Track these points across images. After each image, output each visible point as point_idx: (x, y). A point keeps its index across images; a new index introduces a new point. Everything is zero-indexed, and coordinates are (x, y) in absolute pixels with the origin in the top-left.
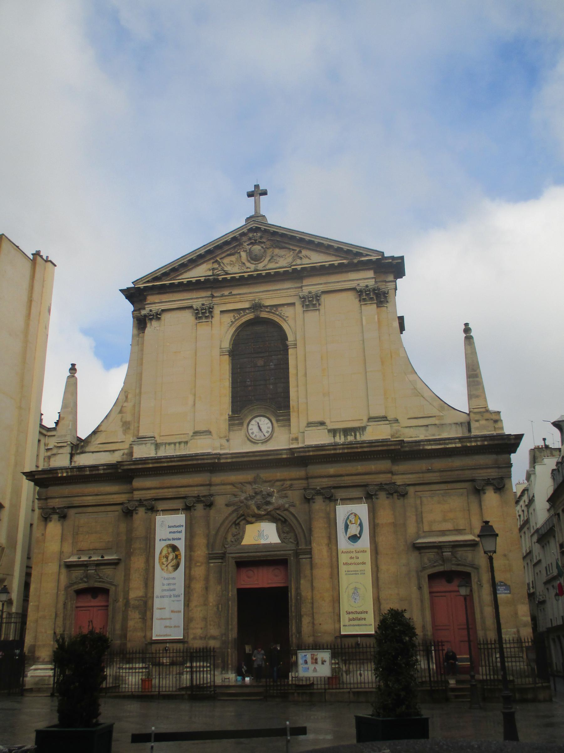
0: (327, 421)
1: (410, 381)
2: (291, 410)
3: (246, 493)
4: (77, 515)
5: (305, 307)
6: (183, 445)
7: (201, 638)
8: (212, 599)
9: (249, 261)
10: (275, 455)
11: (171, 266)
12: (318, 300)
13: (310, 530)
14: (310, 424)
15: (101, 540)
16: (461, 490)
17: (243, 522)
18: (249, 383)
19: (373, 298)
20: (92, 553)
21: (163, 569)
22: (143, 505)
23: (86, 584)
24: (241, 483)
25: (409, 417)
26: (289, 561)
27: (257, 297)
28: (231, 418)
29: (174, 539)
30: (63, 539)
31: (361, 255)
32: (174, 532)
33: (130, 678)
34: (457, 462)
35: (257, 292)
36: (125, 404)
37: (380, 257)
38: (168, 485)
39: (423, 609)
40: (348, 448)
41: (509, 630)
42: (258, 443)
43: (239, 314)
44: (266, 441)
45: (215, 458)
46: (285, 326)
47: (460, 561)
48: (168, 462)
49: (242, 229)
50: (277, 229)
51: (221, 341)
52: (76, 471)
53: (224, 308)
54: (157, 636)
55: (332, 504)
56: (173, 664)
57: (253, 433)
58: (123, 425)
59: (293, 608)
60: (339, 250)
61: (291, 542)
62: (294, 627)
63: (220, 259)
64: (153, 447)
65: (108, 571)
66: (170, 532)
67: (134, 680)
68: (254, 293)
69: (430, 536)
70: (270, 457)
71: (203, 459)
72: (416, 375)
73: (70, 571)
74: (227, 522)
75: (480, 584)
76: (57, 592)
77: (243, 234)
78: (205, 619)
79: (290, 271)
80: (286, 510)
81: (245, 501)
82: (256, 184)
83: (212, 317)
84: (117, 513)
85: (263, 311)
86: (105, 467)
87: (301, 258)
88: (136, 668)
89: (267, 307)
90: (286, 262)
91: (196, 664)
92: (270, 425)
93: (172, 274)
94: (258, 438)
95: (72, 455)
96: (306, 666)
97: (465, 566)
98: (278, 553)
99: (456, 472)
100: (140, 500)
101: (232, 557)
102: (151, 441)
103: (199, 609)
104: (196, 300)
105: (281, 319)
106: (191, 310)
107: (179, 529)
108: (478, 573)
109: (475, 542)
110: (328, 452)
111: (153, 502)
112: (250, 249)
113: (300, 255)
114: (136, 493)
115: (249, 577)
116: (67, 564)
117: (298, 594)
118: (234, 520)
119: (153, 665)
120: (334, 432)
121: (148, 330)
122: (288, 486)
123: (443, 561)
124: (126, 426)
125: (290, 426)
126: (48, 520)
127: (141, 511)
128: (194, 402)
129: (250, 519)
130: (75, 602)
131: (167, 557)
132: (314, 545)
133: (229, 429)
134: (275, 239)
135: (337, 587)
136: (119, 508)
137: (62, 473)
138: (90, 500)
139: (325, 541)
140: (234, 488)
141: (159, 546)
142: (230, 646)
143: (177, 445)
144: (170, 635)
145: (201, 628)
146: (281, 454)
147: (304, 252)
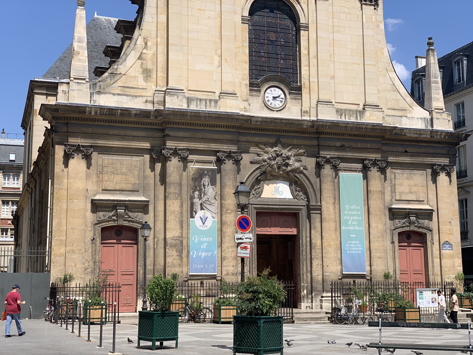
7: (233, 274)
15: (127, 182)
28: (251, 85)
36: (145, 51)
39: (394, 258)
41: (450, 276)
42: (274, 111)
47: (421, 224)
58: (143, 72)
59: (304, 253)
61: (302, 199)
62: (304, 267)
64: (185, 101)
74: (252, 176)
81: (268, 161)
92: (283, 96)
94: (273, 106)
101: (254, 208)
103: (231, 250)
108: (432, 234)
132: (323, 203)
139: (332, 201)
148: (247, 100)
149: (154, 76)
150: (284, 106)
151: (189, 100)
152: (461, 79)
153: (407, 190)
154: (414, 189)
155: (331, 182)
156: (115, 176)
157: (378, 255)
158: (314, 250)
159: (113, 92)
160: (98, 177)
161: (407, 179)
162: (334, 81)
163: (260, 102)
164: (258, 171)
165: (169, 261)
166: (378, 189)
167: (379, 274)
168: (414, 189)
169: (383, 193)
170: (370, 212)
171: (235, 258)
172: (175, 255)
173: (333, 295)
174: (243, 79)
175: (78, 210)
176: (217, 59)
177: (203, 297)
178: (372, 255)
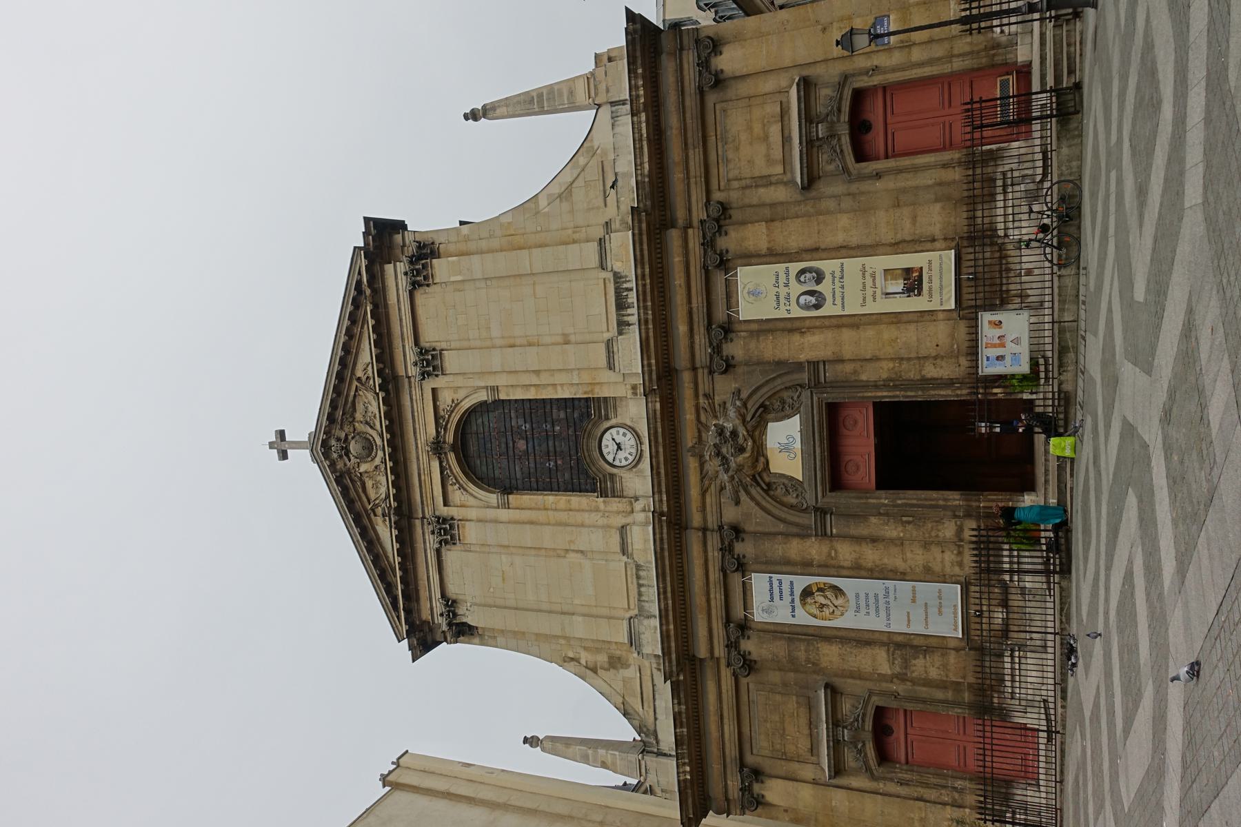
0: (607, 336)
1: (549, 204)
2: (590, 396)
3: (717, 472)
4: (755, 751)
5: (436, 373)
6: (642, 573)
7: (960, 553)
8: (892, 531)
9: (373, 460)
10: (656, 422)
11: (376, 581)
12: (427, 351)
13: (779, 363)
14: (611, 366)
16: (718, 112)
17: (765, 475)
18: (552, 463)
19: (423, 264)
21: (842, 615)
22: (736, 642)
23: (867, 746)
24: (702, 479)
25: (603, 205)
26: (830, 401)
28: (604, 494)
29: (792, 594)
31: (359, 283)
32: (781, 592)
33: (1029, 680)
34: (672, 121)
36: (583, 662)
37: (362, 252)
38: (704, 599)
39: (915, 169)
40: (645, 300)
43: (449, 476)
45: (660, 521)
46: (466, 405)
47: (833, 107)
48: (666, 598)
49: (325, 467)
50: (323, 415)
51: (488, 507)
52: (683, 749)
53: (440, 500)
54: (956, 630)
55: (737, 327)
56: (1005, 604)
57: (626, 459)
58: (614, 668)
59: (909, 393)
60: (353, 319)
61: (798, 397)
62: (942, 393)
64: (646, 622)
65: (846, 706)
66: (781, 599)
67: (1034, 674)
68: (417, 452)
69: (791, 163)
70: (660, 430)
71: (662, 539)
72: (540, 196)
73: (845, 770)
74: (764, 503)
75: (873, 70)
76: (881, 794)
77: (333, 465)
78: (926, 545)
79: (384, 394)
80: (745, 405)
81: (730, 473)
82: (268, 446)
83: (452, 519)
84: (751, 686)
85: (445, 438)
86: (676, 701)
88: (1013, 669)
89: (438, 432)
91: (1006, 563)
92: (613, 431)
93: (389, 579)
94: (634, 451)
95: (660, 754)
96: (1008, 359)
97: (841, 98)
98: (816, 419)
99: (689, 121)
100: (727, 646)
101: (823, 496)
102: (636, 625)
103: (909, 555)
104: (428, 544)
105: (455, 411)
106: (443, 550)
107: (776, 584)
108: (853, 75)
109: (802, 83)
110: (651, 334)
111: (732, 625)
112: (356, 458)
113: (364, 379)
114: (717, 654)
115: (858, 468)
116: (833, 774)
117: (886, 385)
118: (761, 492)
119: (1007, 638)
120: (622, 325)
121: (470, 620)
122: (706, 402)
123: (832, 136)
124: (616, 663)
125: (615, 398)
126: (761, 799)
127: (748, 645)
128: (577, 551)
129: (760, 467)
130: (897, 766)
131: (822, 606)
132: (803, 357)
133: (620, 497)
134: (340, 418)
135: (874, 317)
136: (744, 681)
137: (685, 772)
138: (730, 729)
139: (796, 338)
140: (709, 491)
141: (803, 617)
142: (974, 504)
143: (641, 582)
144: (955, 606)
145: (943, 552)
146: (655, 411)
147: (359, 373)
148: (631, 503)
151: (642, 613)
153: (762, 149)
154: (757, 128)
155: (758, 341)
156: (787, 733)
157: (907, 224)
158: (903, 374)
159: (652, 719)
160: (791, 760)
161: (737, 149)
162: (571, 334)
163: (631, 476)
164: (753, 491)
165: (935, 673)
166: (764, 231)
167: (952, 220)
168: (757, 128)
170: (814, 247)
171: (925, 548)
172: (923, 661)
174: (597, 510)
175: (849, 802)
176: (571, 555)
177: (1007, 613)
178: (908, 238)
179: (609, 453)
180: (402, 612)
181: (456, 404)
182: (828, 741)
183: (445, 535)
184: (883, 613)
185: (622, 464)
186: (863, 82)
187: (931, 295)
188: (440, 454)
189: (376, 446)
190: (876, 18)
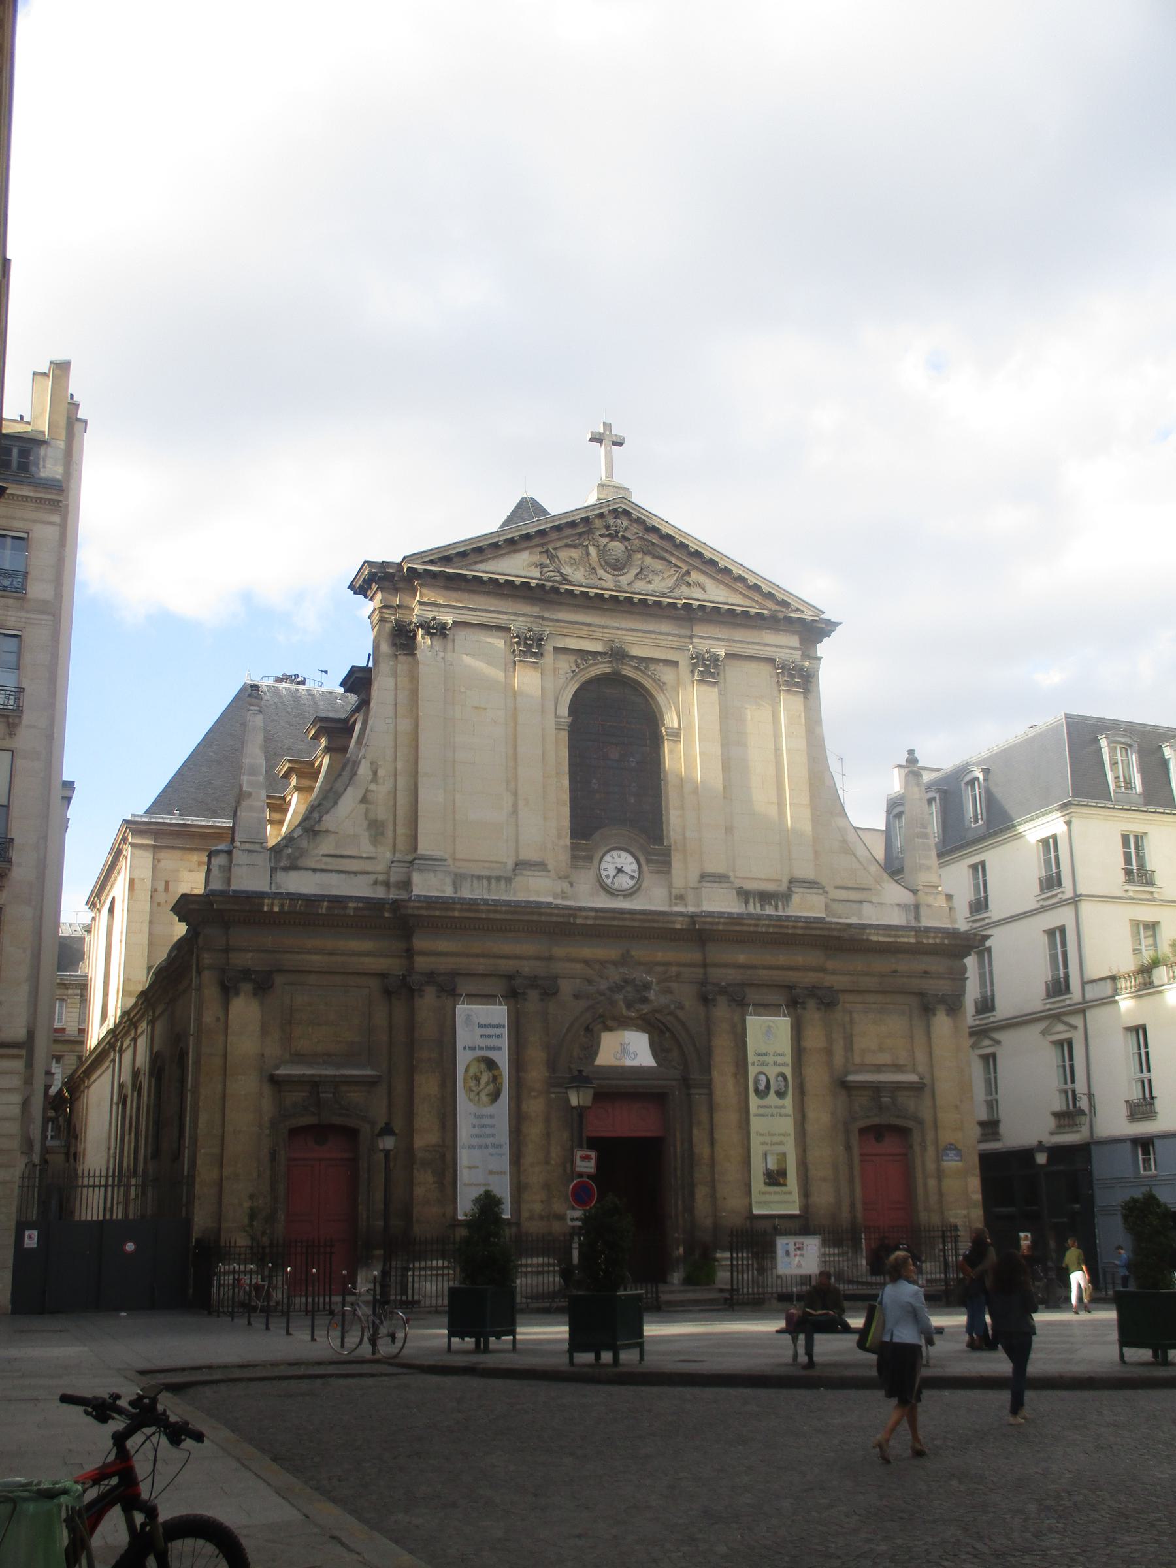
1: (838, 828)
6: (503, 882)
9: (602, 567)
17: (599, 1026)
20: (321, 1061)
21: (471, 1100)
27: (616, 636)
28: (574, 847)
29: (489, 1048)
30: (264, 1031)
32: (489, 1036)
33: (428, 1285)
35: (618, 629)
36: (373, 787)
44: (629, 894)
45: (570, 915)
49: (602, 508)
62: (680, 1202)
63: (553, 549)
64: (448, 880)
66: (482, 1036)
67: (434, 1288)
68: (613, 628)
70: (655, 925)
71: (551, 915)
77: (601, 516)
78: (547, 1186)
80: (671, 1013)
85: (626, 664)
86: (360, 905)
87: (689, 585)
88: (431, 1268)
90: (663, 584)
92: (635, 866)
94: (616, 886)
96: (787, 1259)
107: (498, 1031)
112: (605, 546)
113: (688, 579)
120: (745, 895)
125: (669, 872)
128: (515, 805)
129: (610, 1023)
131: (477, 1079)
132: (715, 1074)
134: (649, 538)
137: (273, 904)
141: (463, 1059)
145: (542, 1202)
147: (695, 576)
148: (567, 877)
149: (390, 833)
150: (637, 886)
151: (458, 879)
152: (979, 817)
159: (313, 865)
169: (829, 1052)
173: (735, 1255)
174: (559, 837)
179: (613, 858)
180: (440, 569)
181: (662, 686)
182: (320, 1076)
183: (525, 643)
184: (475, 1141)
185: (602, 871)
186: (916, 1138)
187: (764, 1193)
188: (611, 656)
189: (618, 576)
190: (960, 1150)
